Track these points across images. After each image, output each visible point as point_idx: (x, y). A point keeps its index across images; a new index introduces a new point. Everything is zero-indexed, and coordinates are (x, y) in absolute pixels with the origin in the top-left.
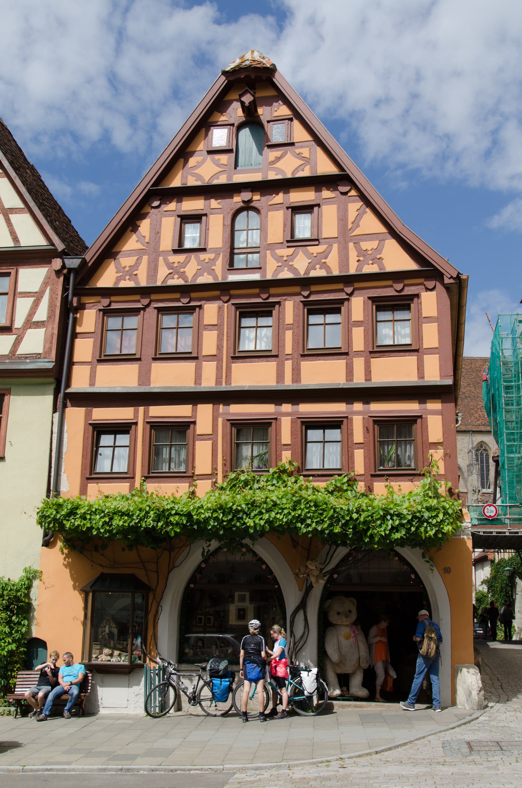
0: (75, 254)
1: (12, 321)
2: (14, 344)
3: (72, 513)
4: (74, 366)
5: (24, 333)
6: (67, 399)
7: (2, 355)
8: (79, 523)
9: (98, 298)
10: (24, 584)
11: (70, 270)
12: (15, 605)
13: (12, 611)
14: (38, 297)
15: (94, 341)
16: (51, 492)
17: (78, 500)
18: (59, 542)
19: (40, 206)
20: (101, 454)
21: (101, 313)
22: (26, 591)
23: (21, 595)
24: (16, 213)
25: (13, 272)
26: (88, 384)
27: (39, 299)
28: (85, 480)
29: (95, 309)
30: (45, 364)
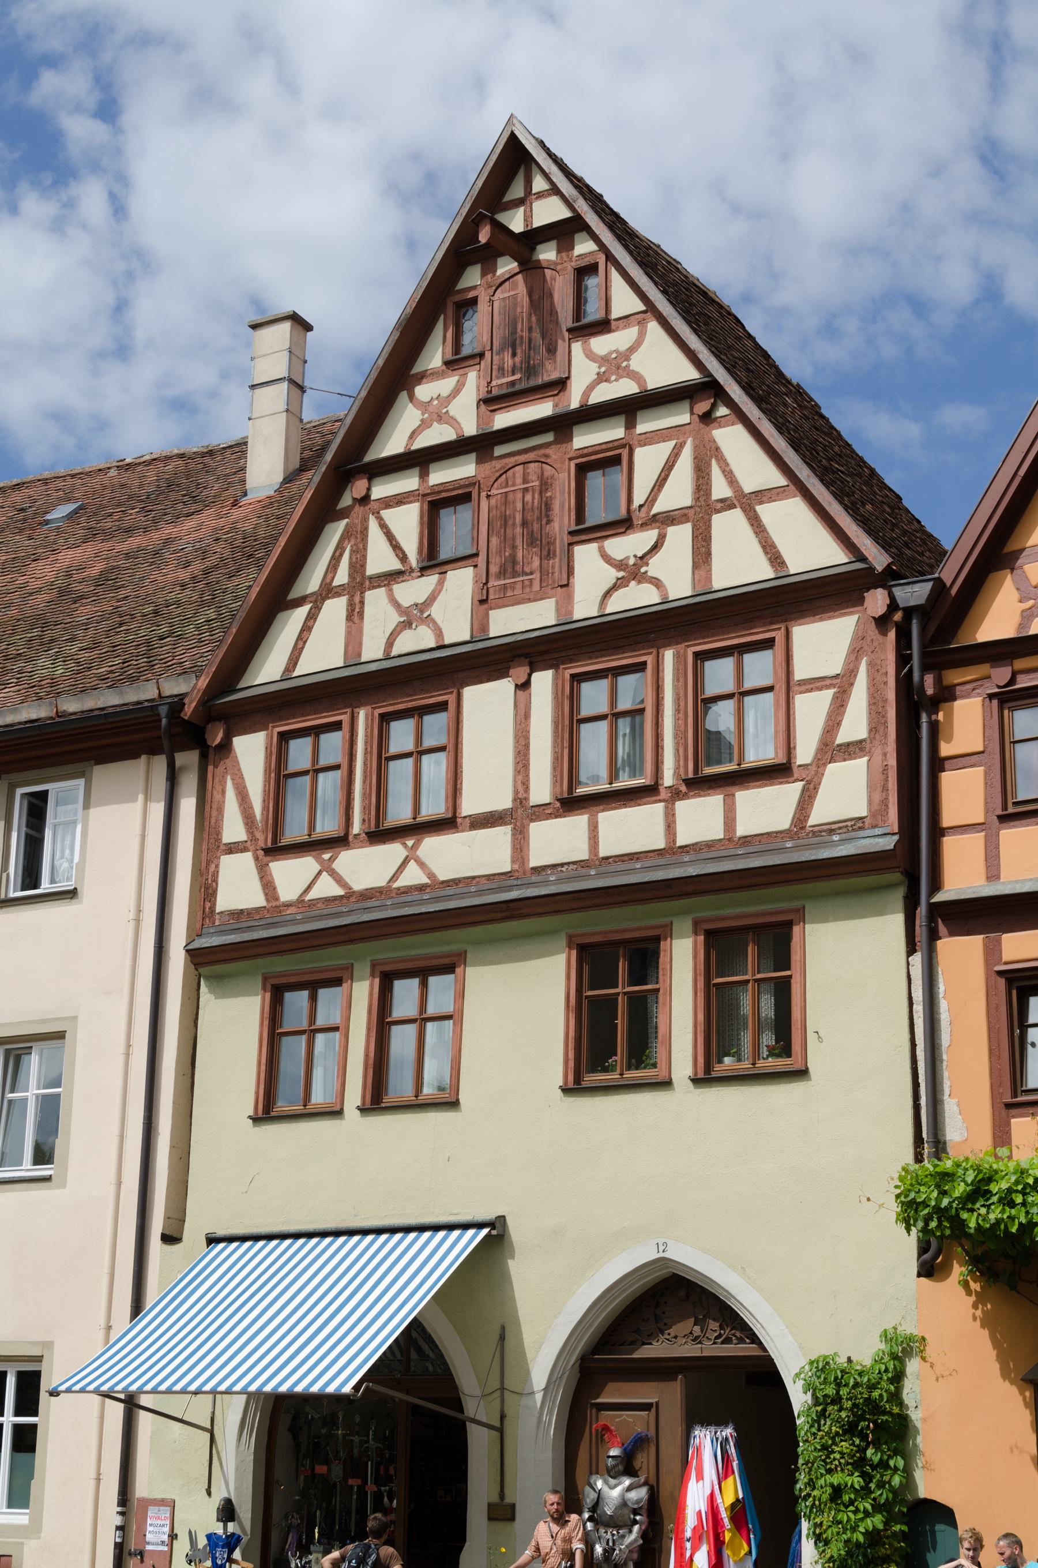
3: (979, 1191)
4: (945, 839)
5: (819, 775)
6: (937, 918)
8: (1000, 1216)
9: (983, 669)
10: (886, 1370)
11: (909, 612)
12: (869, 1420)
14: (841, 685)
15: (985, 772)
16: (926, 1145)
17: (991, 1159)
20: (1033, 1045)
21: (995, 702)
23: (881, 1395)
24: (771, 500)
25: (779, 636)
26: (984, 877)
27: (844, 691)
28: (1004, 1111)
29: (979, 695)
30: (877, 840)
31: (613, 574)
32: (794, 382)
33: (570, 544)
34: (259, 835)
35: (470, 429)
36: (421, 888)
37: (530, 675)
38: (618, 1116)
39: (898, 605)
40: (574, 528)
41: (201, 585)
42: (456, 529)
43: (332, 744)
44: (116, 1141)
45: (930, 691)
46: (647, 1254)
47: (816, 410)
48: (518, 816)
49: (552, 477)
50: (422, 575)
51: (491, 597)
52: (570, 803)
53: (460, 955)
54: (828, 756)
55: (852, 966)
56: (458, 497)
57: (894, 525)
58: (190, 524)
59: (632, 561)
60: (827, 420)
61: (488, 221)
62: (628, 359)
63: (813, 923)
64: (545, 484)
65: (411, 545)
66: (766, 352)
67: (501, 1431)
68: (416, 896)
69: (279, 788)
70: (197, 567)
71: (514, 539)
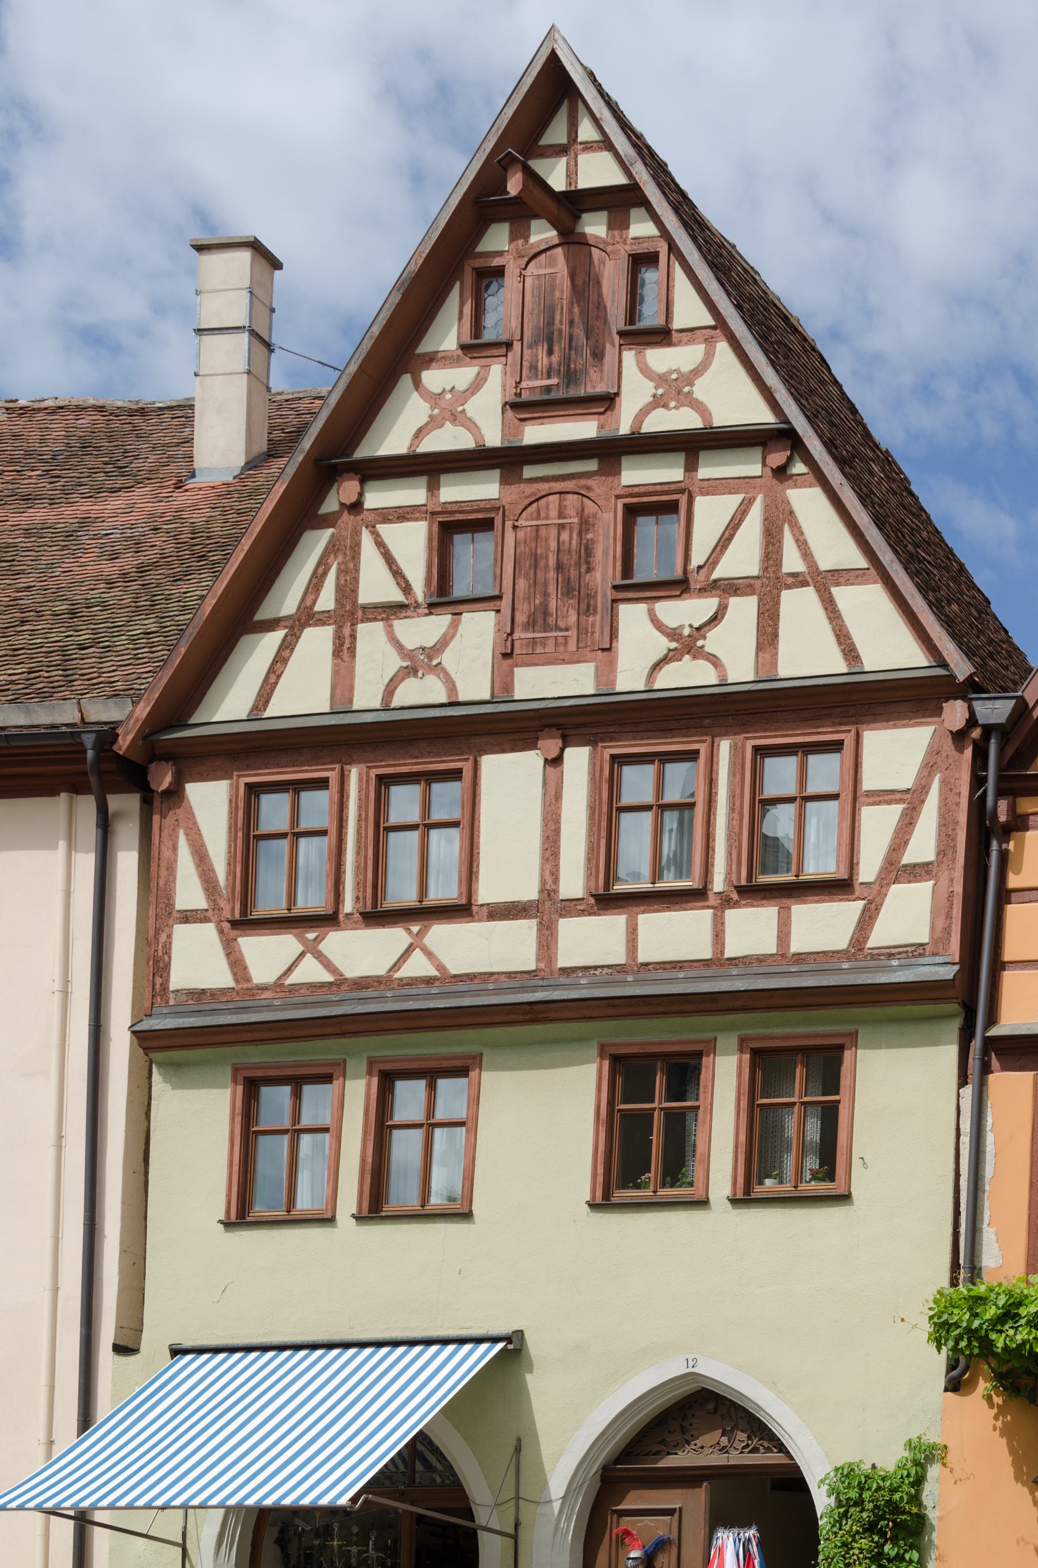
0: (1001, 687)
1: (852, 865)
2: (859, 922)
3: (1009, 1315)
4: (1005, 973)
6: (992, 1052)
7: (833, 952)
8: (1026, 1337)
10: (908, 1476)
12: (889, 1520)
13: (882, 1534)
14: (911, 801)
16: (962, 1271)
17: (1023, 1285)
18: (981, 1381)
19: (908, 562)
22: (913, 1491)
23: (901, 1498)
24: (848, 583)
25: (849, 739)
27: (914, 808)
30: (937, 968)
31: (663, 644)
32: (883, 447)
33: (614, 601)
34: (223, 904)
35: (493, 439)
36: (429, 981)
37: (562, 750)
38: (649, 1235)
39: (977, 721)
40: (619, 582)
41: (135, 586)
42: (474, 562)
43: (316, 806)
44: (48, 1243)
45: (1003, 818)
46: (675, 1368)
47: (904, 485)
48: (546, 909)
49: (595, 515)
50: (431, 613)
51: (517, 651)
52: (606, 900)
53: (474, 1057)
54: (893, 876)
55: (901, 1094)
56: (478, 522)
57: (980, 631)
58: (116, 503)
59: (686, 632)
60: (917, 499)
61: (520, 167)
62: (691, 384)
63: (865, 1048)
64: (586, 524)
65: (417, 573)
66: (853, 405)
67: (515, 1538)
68: (422, 989)
69: (248, 850)
70: (128, 561)
71: (546, 584)
